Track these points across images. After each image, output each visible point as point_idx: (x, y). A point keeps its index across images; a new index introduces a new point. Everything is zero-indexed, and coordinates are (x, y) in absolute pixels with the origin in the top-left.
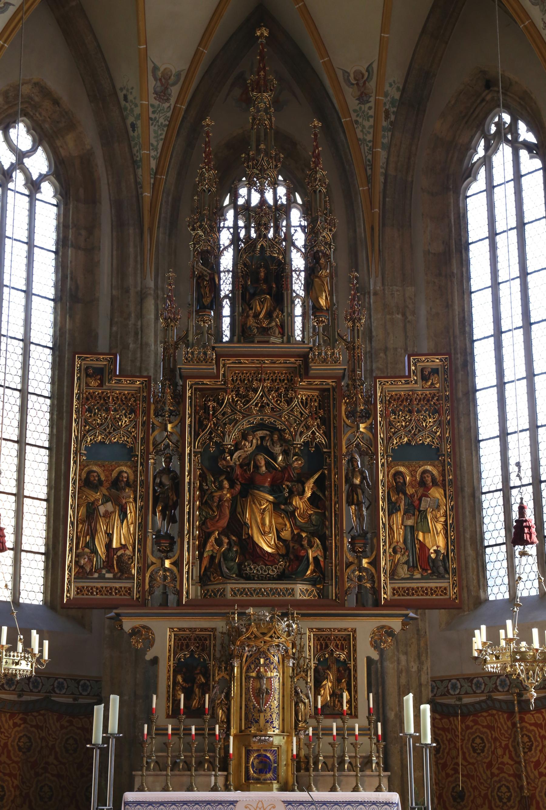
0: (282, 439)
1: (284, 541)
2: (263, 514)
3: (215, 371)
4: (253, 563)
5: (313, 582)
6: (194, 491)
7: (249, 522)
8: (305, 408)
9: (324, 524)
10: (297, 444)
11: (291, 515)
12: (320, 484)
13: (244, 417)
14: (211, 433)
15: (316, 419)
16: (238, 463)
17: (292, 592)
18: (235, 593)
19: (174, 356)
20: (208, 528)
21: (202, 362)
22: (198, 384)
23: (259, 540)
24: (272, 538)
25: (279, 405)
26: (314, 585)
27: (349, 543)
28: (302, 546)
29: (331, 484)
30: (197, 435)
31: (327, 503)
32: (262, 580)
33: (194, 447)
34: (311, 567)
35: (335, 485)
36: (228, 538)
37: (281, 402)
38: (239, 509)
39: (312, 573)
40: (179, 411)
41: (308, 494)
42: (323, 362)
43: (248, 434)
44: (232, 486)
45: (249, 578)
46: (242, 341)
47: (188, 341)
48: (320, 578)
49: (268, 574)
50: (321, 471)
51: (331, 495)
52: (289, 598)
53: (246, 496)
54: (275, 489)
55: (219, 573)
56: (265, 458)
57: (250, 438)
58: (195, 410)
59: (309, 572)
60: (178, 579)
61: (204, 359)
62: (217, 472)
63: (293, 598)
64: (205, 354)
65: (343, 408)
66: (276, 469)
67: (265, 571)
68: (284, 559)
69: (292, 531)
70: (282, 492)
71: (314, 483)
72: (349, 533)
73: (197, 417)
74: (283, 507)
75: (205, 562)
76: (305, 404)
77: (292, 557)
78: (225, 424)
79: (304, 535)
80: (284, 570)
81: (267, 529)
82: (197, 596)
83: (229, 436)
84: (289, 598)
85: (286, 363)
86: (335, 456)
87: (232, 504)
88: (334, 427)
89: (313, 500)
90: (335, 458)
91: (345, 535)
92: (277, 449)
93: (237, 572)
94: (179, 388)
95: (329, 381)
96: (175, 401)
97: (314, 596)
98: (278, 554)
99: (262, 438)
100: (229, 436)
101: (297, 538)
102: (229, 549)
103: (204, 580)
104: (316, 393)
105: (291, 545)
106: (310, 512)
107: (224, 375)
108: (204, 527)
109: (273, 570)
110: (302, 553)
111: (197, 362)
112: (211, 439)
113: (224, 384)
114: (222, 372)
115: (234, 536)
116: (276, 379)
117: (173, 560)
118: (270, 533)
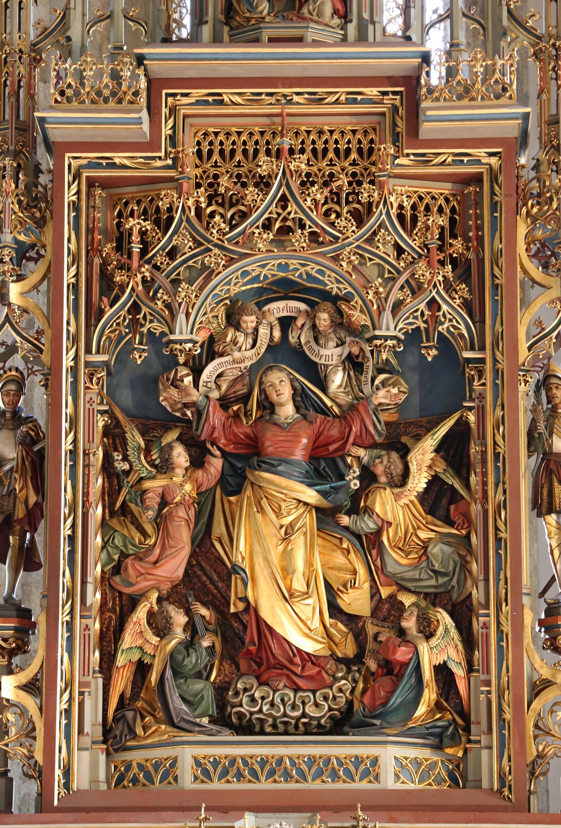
0: (341, 323)
1: (351, 620)
2: (287, 537)
3: (146, 127)
4: (261, 684)
5: (438, 740)
6: (87, 476)
7: (246, 565)
8: (410, 236)
9: (464, 566)
10: (386, 338)
11: (370, 544)
12: (455, 450)
13: (231, 261)
14: (135, 308)
15: (442, 263)
16: (215, 395)
17: (371, 769)
18: (206, 773)
19: (30, 87)
20: (131, 585)
21: (106, 100)
22: (99, 166)
23: (274, 615)
24: (312, 608)
25: (332, 225)
26: (438, 747)
27: (541, 623)
28: (402, 632)
29: (484, 453)
30: (94, 314)
31: (475, 509)
32: (286, 733)
33: (88, 351)
34: (430, 695)
35: (497, 456)
36: (188, 612)
37: (338, 216)
38: (219, 528)
39: (431, 712)
40: (44, 246)
41: (419, 482)
42: (460, 97)
43: (243, 311)
44: (198, 461)
45: (245, 727)
46: (226, 37)
47: (69, 39)
48: (454, 725)
49: (304, 715)
50: (455, 417)
51: (485, 484)
52: (364, 785)
53: (238, 491)
54: (323, 466)
55: (160, 714)
56: (293, 380)
57: (249, 321)
58: (90, 243)
59: (422, 709)
60: (40, 733)
61: (114, 94)
62: (155, 423)
63: (375, 786)
64: (116, 76)
65: (522, 229)
66: (324, 411)
67: (294, 707)
68: (349, 671)
69: (374, 592)
70: (342, 477)
71: (437, 450)
72: (542, 594)
73: (97, 261)
74: (345, 520)
75: (122, 682)
76: (408, 220)
77: (373, 665)
78: (176, 282)
79: (407, 600)
80: (350, 703)
81: (299, 585)
82: (94, 781)
83: (188, 315)
84: (364, 785)
85: (355, 101)
86: (496, 371)
87: (198, 515)
88: (495, 287)
89: (438, 500)
90: (496, 377)
91: (525, 600)
92: (329, 354)
93: (213, 710)
94: (43, 179)
95: (480, 152)
96: (32, 217)
97: (439, 781)
98: (333, 655)
99: (286, 323)
100: (188, 315)
101: (388, 611)
102: (190, 644)
103: (115, 734)
104: (446, 188)
105: (371, 629)
106: (423, 535)
107: (172, 139)
108: (117, 579)
109: (317, 705)
110: (402, 654)
111: (93, 102)
112: (135, 325)
113: (173, 167)
114: (166, 131)
115: (205, 604)
116: (325, 151)
117: (24, 677)
118: (306, 594)
